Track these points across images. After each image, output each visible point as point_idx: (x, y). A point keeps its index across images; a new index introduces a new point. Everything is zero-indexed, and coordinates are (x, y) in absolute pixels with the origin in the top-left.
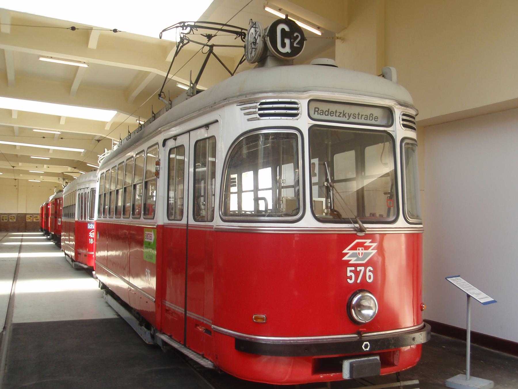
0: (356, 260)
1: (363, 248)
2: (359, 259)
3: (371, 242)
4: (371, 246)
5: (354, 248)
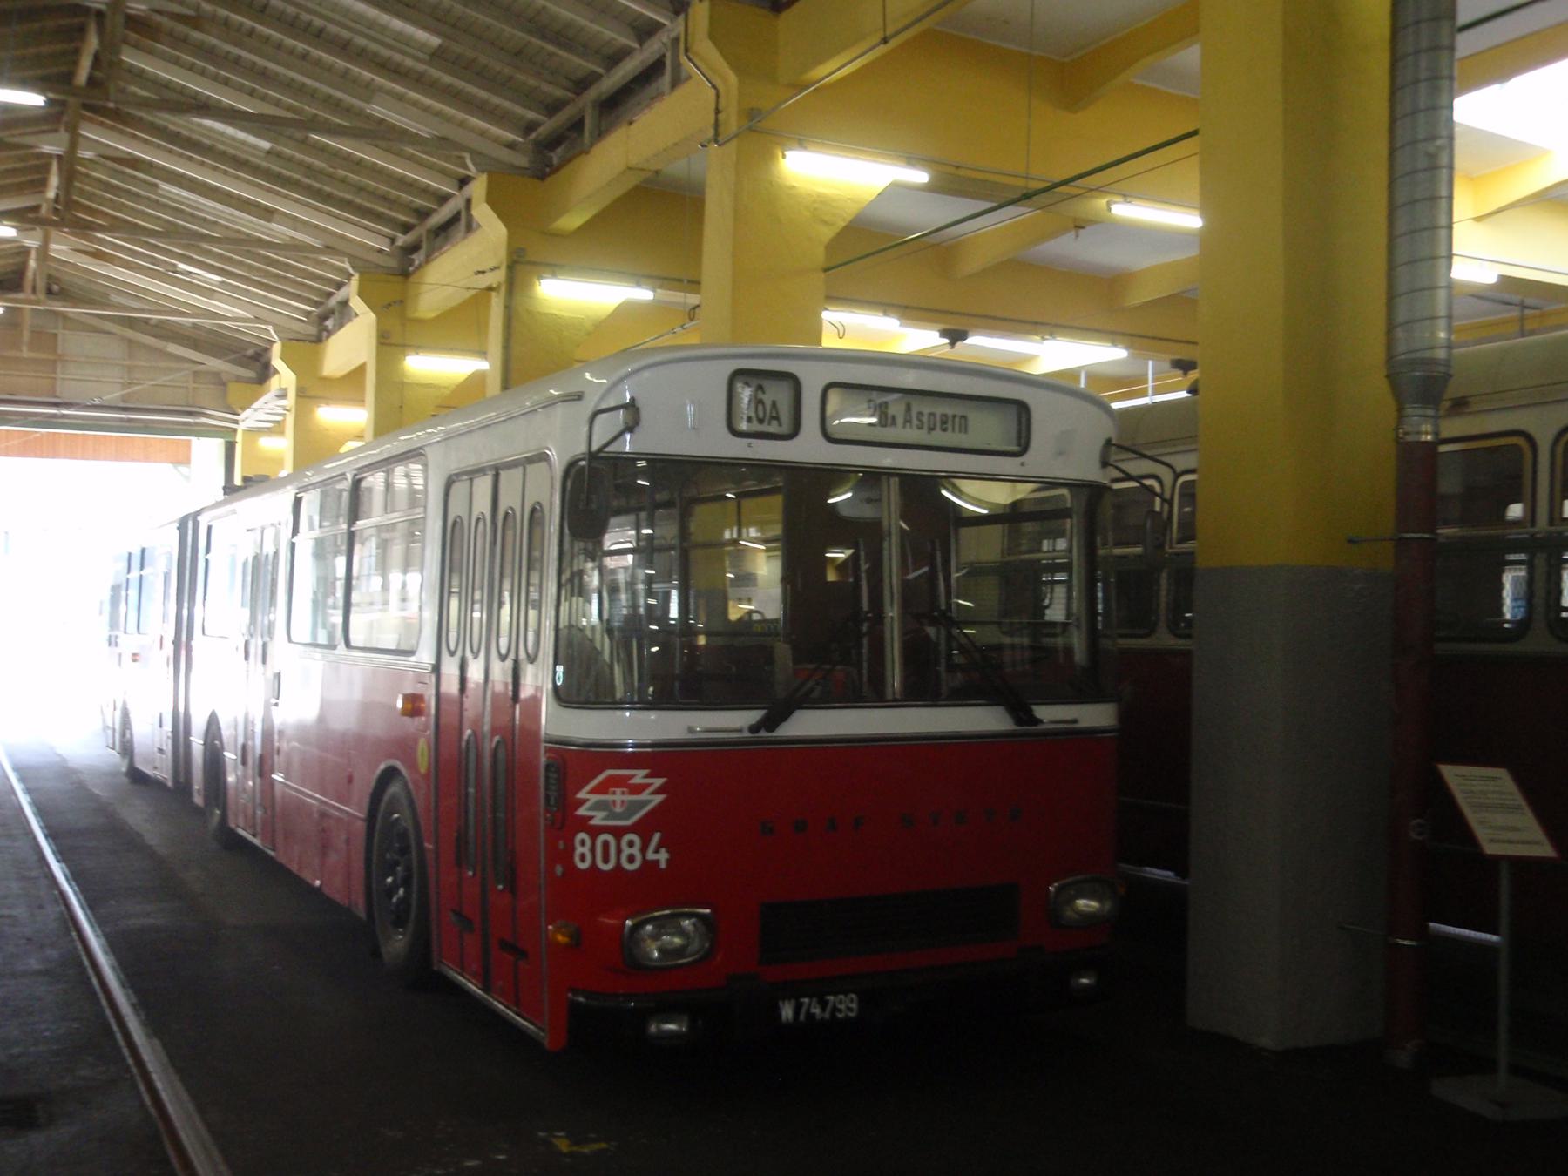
0: (604, 819)
1: (625, 790)
2: (613, 816)
3: (647, 776)
4: (648, 786)
5: (601, 789)
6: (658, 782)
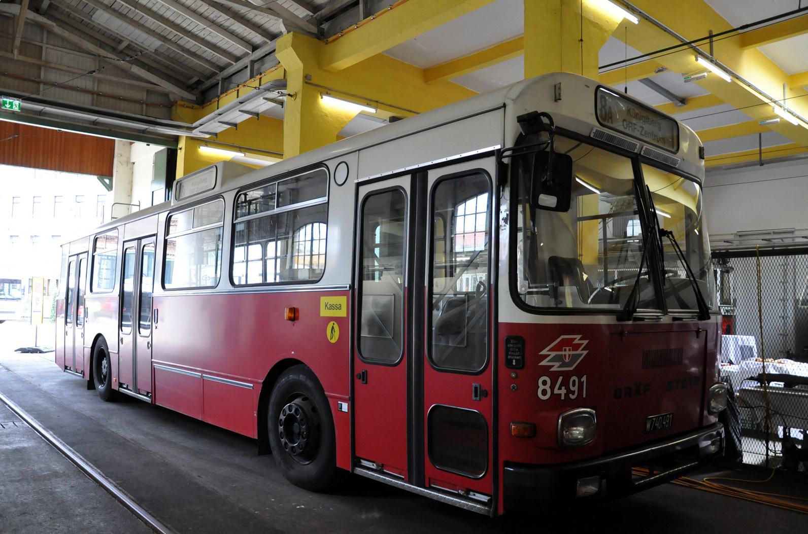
5: (558, 348)
6: (585, 342)
